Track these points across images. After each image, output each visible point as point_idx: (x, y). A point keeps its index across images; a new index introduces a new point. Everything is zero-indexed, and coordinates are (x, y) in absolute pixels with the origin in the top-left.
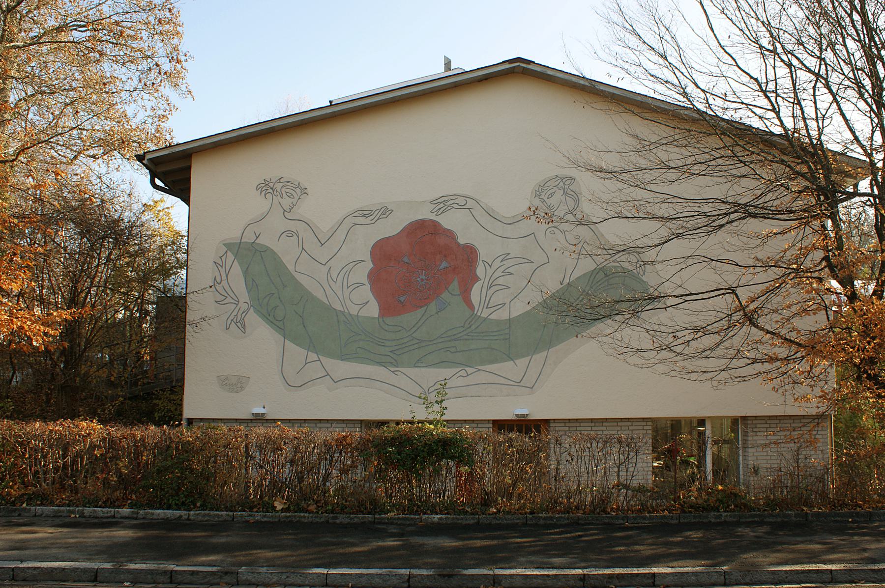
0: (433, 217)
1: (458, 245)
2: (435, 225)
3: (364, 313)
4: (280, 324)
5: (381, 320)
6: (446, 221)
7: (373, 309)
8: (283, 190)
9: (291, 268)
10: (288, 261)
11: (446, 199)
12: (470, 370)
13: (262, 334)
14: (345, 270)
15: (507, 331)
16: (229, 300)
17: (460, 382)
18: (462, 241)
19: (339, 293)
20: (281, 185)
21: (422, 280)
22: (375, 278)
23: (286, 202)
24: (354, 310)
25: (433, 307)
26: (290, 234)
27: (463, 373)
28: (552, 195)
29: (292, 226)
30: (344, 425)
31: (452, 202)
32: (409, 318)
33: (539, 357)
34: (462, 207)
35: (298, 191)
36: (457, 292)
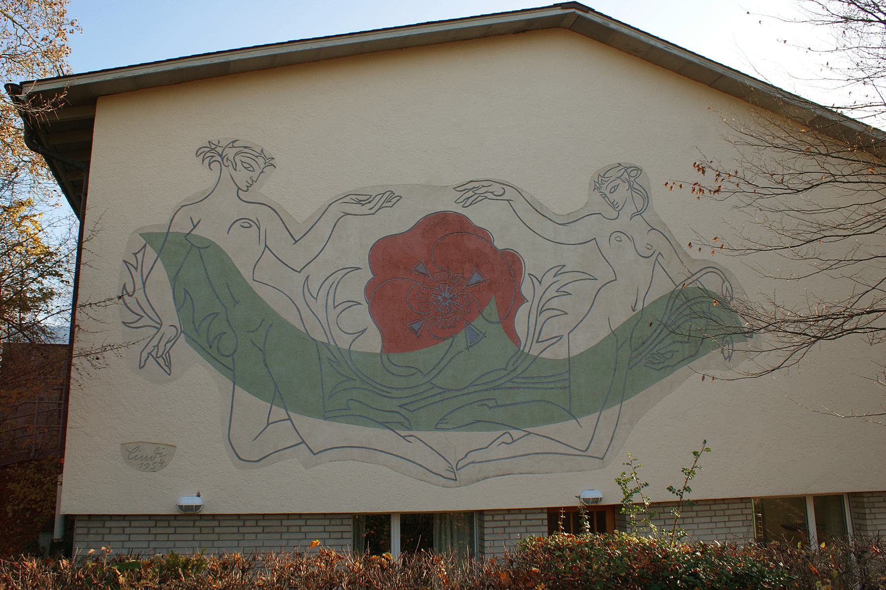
1: (495, 250)
2: (462, 220)
5: (385, 357)
6: (480, 216)
8: (238, 158)
9: (247, 274)
10: (243, 264)
11: (476, 184)
12: (516, 434)
14: (330, 280)
15: (566, 376)
17: (502, 451)
18: (499, 245)
19: (322, 315)
20: (235, 150)
22: (376, 294)
23: (242, 177)
24: (343, 342)
25: (461, 339)
26: (247, 223)
28: (614, 189)
29: (250, 212)
30: (327, 522)
31: (484, 190)
32: (427, 356)
33: (610, 413)
34: (499, 197)
35: (261, 161)
36: (495, 318)
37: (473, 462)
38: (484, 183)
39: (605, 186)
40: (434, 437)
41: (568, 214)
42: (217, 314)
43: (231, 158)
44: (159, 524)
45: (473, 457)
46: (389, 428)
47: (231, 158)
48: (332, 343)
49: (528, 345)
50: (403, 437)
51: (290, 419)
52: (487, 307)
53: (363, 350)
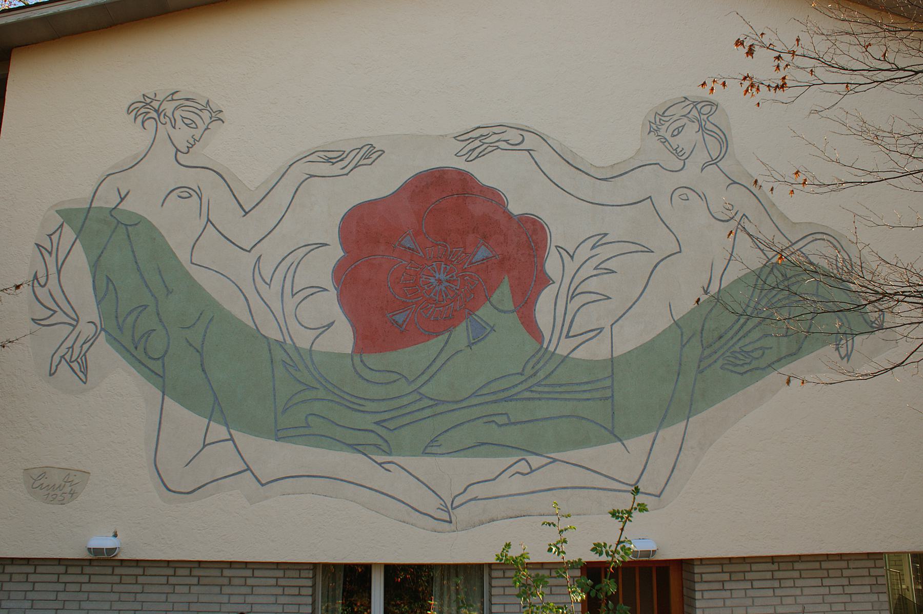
0: (460, 164)
1: (509, 216)
3: (326, 344)
4: (156, 366)
5: (357, 359)
6: (486, 172)
7: (342, 338)
8: (177, 114)
9: (183, 256)
13: (120, 385)
15: (608, 383)
16: (59, 317)
17: (517, 484)
18: (516, 208)
19: (276, 306)
21: (440, 281)
22: (349, 279)
23: (182, 135)
24: (303, 340)
25: (461, 333)
26: (186, 192)
27: (522, 467)
28: (679, 131)
29: (190, 178)
30: (280, 573)
32: (414, 357)
33: (671, 434)
34: (515, 147)
36: (509, 305)
37: (475, 499)
38: (496, 130)
39: (664, 128)
40: (421, 465)
41: (612, 166)
42: (146, 306)
43: (169, 114)
44: (70, 570)
45: (475, 491)
46: (359, 451)
47: (169, 114)
48: (289, 341)
49: (554, 341)
50: (380, 464)
51: (232, 439)
52: (497, 292)
53: (329, 350)
